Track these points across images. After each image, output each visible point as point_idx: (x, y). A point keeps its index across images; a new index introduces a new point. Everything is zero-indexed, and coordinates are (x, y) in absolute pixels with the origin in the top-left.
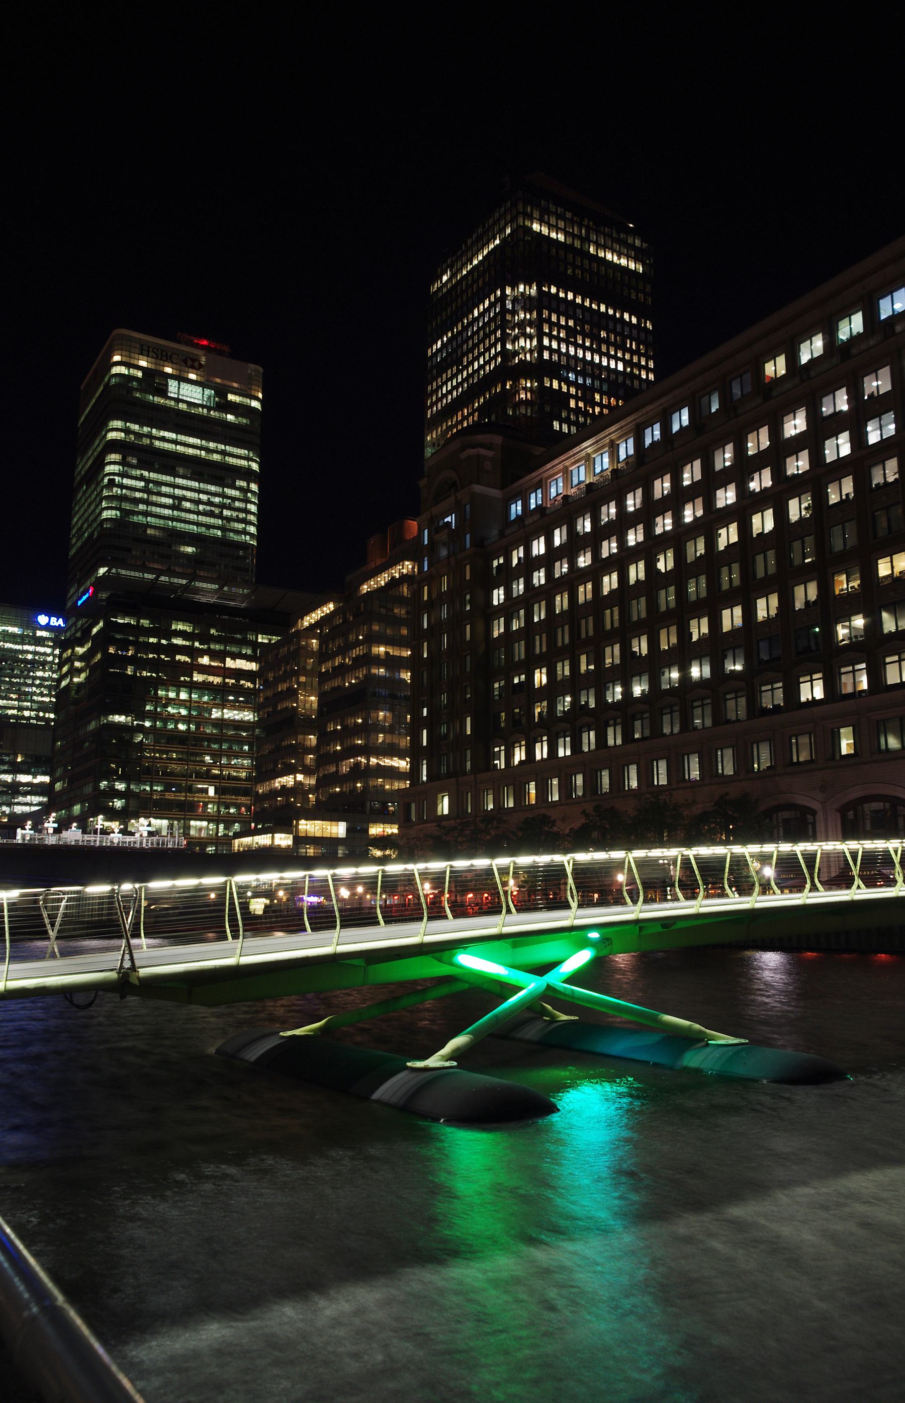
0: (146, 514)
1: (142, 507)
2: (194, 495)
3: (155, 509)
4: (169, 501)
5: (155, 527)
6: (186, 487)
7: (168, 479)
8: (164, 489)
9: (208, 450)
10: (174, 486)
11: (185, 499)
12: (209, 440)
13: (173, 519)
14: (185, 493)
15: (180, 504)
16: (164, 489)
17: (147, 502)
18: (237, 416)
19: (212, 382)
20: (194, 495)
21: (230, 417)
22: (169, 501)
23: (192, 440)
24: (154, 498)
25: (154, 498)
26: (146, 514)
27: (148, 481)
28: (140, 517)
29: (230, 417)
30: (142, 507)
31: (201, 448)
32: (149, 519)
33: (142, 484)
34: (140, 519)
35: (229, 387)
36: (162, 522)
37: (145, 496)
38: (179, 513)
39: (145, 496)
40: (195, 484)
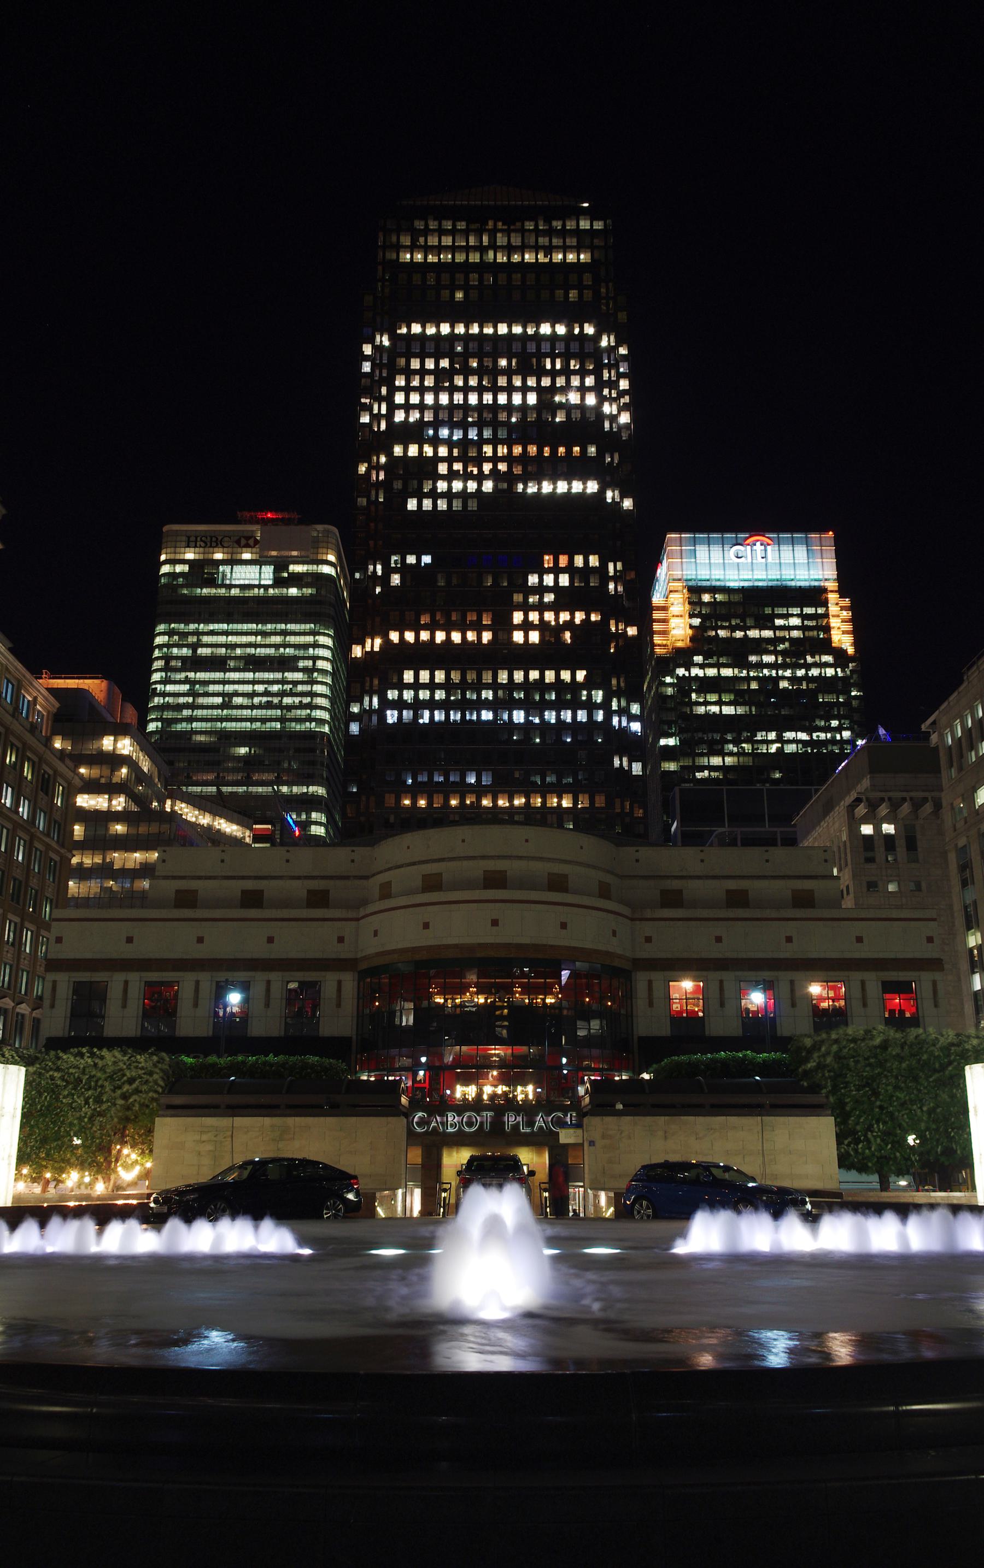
0: (191, 719)
1: (186, 713)
2: (248, 688)
3: (199, 713)
4: (219, 700)
5: (201, 733)
6: (240, 682)
7: (218, 675)
8: (212, 688)
9: (264, 634)
10: (224, 682)
11: (236, 694)
12: (264, 622)
13: (221, 720)
14: (236, 687)
15: (230, 701)
16: (212, 688)
17: (192, 707)
18: (300, 587)
19: (267, 557)
20: (248, 688)
21: (293, 591)
22: (219, 700)
23: (245, 627)
24: (201, 700)
25: (201, 700)
26: (191, 719)
27: (193, 683)
28: (184, 724)
29: (293, 591)
30: (186, 713)
31: (256, 634)
32: (194, 725)
33: (187, 687)
34: (180, 727)
35: (287, 557)
36: (209, 725)
37: (190, 700)
38: (230, 712)
39: (190, 700)
40: (249, 676)
